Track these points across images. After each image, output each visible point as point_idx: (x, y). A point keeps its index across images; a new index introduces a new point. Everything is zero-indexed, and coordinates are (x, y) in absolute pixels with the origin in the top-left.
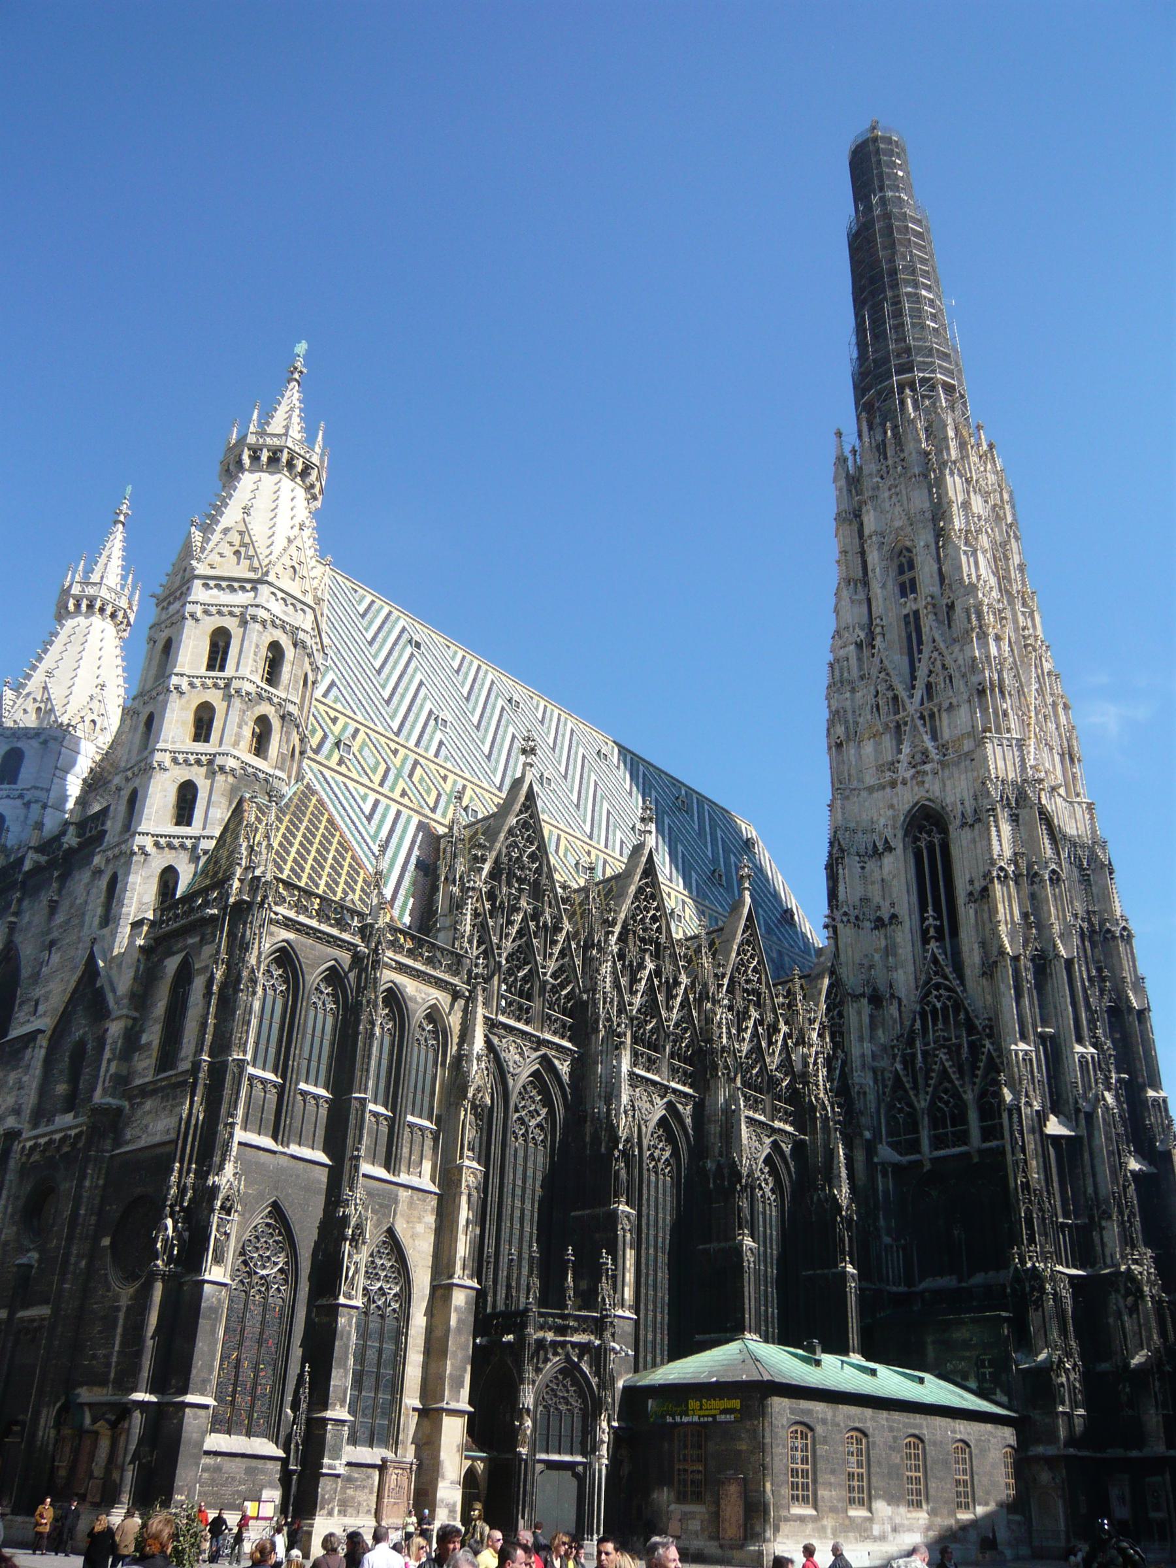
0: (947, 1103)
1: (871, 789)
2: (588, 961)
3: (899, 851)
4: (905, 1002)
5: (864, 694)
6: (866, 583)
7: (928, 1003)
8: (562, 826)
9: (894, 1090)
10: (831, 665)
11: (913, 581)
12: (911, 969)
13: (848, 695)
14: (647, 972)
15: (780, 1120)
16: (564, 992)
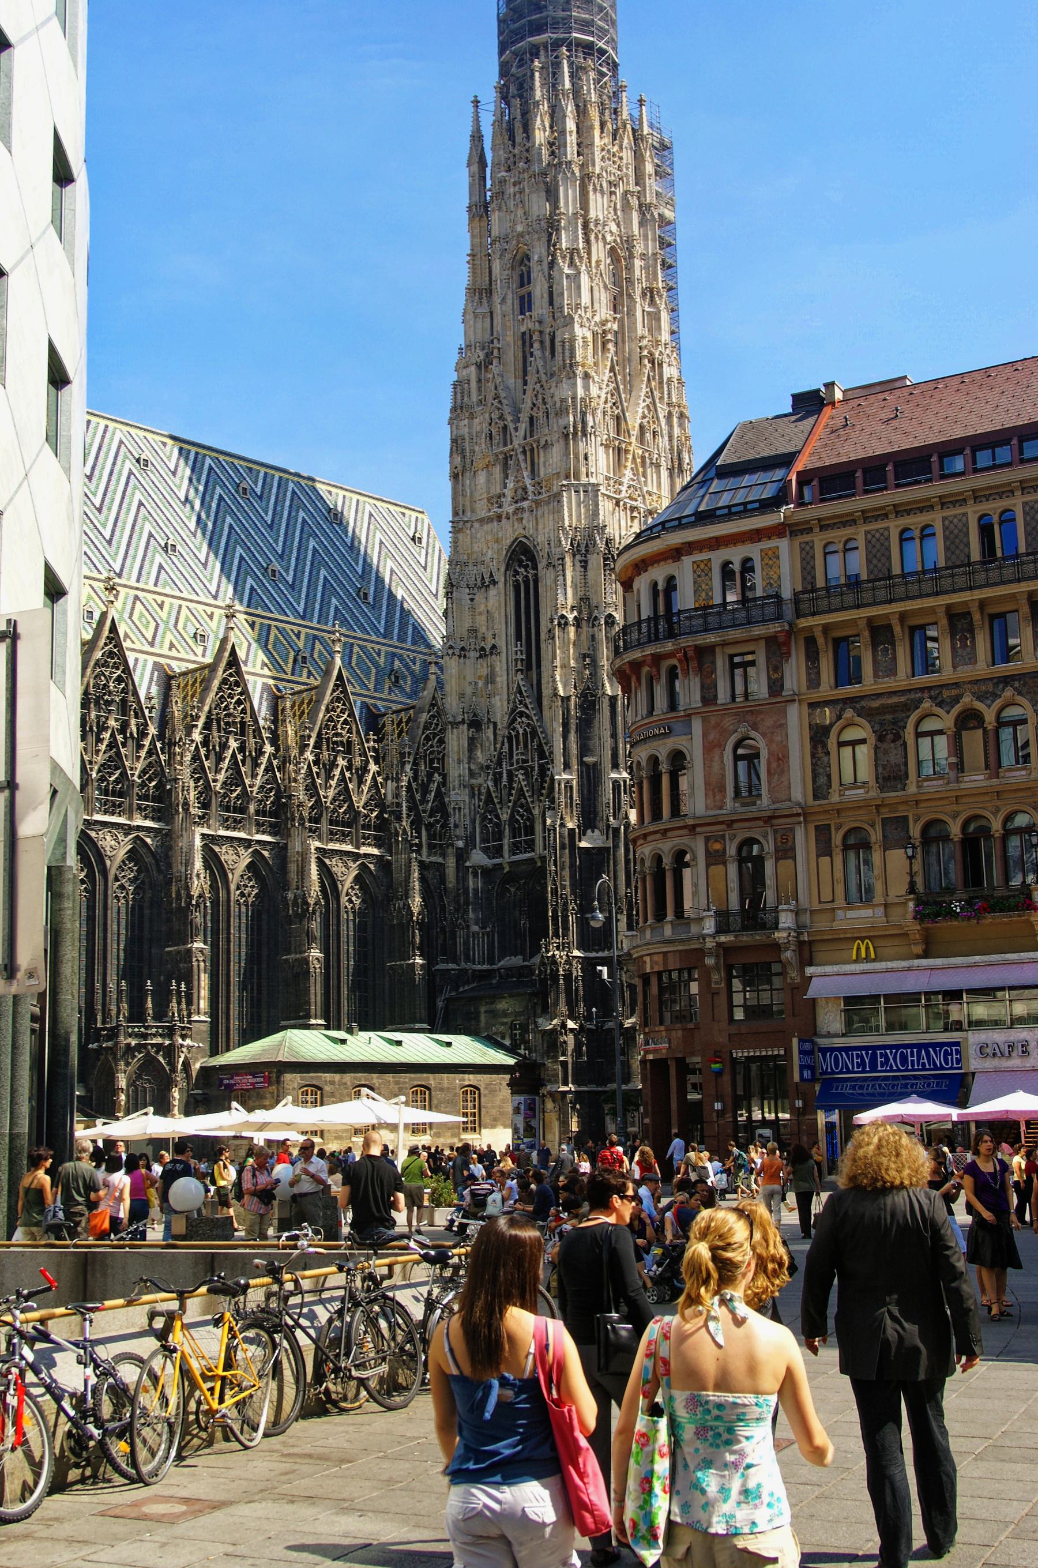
0: (522, 816)
1: (481, 521)
2: (171, 756)
3: (501, 585)
4: (499, 726)
5: (480, 423)
6: (490, 292)
7: (514, 729)
8: (185, 595)
9: (486, 803)
10: (455, 385)
11: (529, 294)
12: (505, 697)
13: (466, 422)
14: (231, 751)
15: (369, 845)
16: (154, 783)
